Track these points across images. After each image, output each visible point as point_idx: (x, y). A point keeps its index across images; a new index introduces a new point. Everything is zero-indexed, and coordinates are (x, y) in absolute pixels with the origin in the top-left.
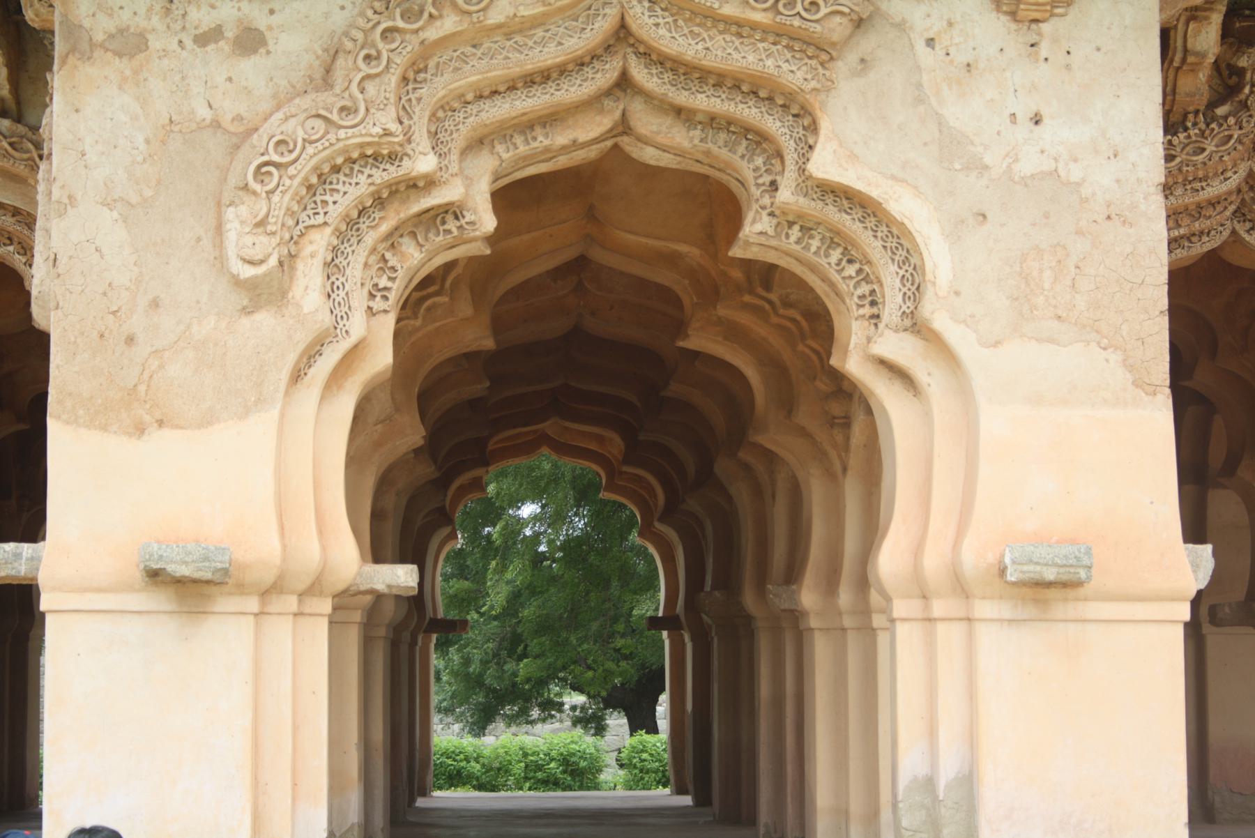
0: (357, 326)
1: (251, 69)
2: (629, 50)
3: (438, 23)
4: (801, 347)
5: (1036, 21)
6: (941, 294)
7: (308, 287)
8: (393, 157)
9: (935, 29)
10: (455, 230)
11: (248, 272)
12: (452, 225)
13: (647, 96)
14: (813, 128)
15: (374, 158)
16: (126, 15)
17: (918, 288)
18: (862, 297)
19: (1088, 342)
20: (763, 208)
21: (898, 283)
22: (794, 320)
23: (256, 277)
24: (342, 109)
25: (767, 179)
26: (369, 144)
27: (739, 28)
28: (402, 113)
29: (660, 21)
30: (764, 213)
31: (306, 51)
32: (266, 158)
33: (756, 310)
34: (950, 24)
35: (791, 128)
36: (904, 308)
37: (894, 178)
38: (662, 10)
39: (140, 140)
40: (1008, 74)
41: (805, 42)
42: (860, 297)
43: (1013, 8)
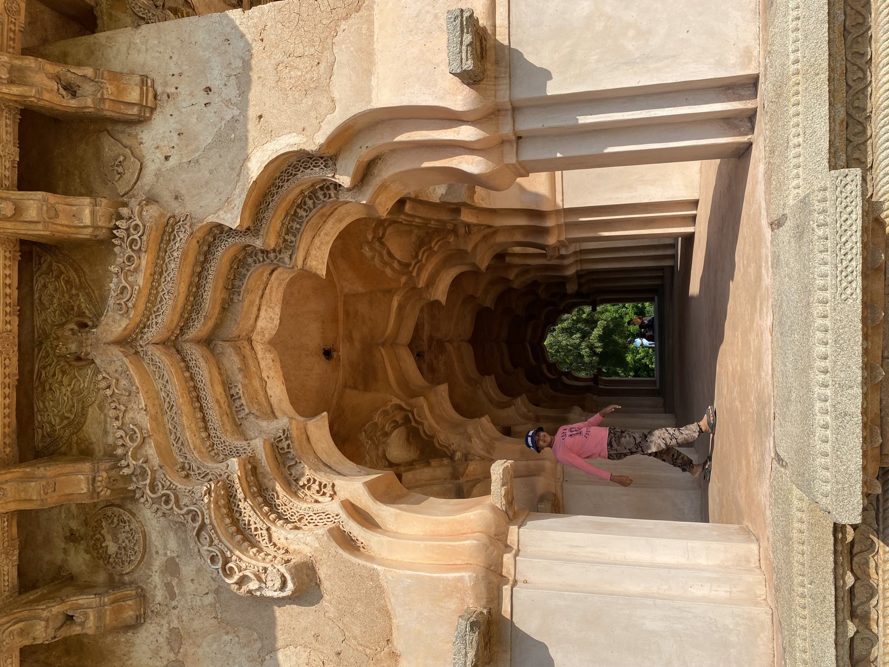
0: (333, 507)
1: (187, 570)
2: (180, 339)
3: (150, 457)
4: (435, 249)
5: (155, 96)
6: (305, 140)
7: (304, 542)
10: (287, 442)
11: (290, 586)
12: (284, 444)
13: (217, 326)
14: (219, 226)
16: (161, 640)
19: (333, 43)
20: (276, 257)
21: (308, 171)
22: (424, 253)
23: (293, 579)
24: (194, 520)
25: (260, 255)
26: (216, 503)
27: (158, 273)
28: (206, 479)
29: (154, 321)
31: (176, 534)
32: (220, 571)
33: (420, 270)
34: (157, 147)
36: (322, 166)
37: (239, 175)
38: (148, 320)
39: (226, 638)
40: (184, 110)
41: (164, 233)
42: (325, 197)
43: (147, 110)
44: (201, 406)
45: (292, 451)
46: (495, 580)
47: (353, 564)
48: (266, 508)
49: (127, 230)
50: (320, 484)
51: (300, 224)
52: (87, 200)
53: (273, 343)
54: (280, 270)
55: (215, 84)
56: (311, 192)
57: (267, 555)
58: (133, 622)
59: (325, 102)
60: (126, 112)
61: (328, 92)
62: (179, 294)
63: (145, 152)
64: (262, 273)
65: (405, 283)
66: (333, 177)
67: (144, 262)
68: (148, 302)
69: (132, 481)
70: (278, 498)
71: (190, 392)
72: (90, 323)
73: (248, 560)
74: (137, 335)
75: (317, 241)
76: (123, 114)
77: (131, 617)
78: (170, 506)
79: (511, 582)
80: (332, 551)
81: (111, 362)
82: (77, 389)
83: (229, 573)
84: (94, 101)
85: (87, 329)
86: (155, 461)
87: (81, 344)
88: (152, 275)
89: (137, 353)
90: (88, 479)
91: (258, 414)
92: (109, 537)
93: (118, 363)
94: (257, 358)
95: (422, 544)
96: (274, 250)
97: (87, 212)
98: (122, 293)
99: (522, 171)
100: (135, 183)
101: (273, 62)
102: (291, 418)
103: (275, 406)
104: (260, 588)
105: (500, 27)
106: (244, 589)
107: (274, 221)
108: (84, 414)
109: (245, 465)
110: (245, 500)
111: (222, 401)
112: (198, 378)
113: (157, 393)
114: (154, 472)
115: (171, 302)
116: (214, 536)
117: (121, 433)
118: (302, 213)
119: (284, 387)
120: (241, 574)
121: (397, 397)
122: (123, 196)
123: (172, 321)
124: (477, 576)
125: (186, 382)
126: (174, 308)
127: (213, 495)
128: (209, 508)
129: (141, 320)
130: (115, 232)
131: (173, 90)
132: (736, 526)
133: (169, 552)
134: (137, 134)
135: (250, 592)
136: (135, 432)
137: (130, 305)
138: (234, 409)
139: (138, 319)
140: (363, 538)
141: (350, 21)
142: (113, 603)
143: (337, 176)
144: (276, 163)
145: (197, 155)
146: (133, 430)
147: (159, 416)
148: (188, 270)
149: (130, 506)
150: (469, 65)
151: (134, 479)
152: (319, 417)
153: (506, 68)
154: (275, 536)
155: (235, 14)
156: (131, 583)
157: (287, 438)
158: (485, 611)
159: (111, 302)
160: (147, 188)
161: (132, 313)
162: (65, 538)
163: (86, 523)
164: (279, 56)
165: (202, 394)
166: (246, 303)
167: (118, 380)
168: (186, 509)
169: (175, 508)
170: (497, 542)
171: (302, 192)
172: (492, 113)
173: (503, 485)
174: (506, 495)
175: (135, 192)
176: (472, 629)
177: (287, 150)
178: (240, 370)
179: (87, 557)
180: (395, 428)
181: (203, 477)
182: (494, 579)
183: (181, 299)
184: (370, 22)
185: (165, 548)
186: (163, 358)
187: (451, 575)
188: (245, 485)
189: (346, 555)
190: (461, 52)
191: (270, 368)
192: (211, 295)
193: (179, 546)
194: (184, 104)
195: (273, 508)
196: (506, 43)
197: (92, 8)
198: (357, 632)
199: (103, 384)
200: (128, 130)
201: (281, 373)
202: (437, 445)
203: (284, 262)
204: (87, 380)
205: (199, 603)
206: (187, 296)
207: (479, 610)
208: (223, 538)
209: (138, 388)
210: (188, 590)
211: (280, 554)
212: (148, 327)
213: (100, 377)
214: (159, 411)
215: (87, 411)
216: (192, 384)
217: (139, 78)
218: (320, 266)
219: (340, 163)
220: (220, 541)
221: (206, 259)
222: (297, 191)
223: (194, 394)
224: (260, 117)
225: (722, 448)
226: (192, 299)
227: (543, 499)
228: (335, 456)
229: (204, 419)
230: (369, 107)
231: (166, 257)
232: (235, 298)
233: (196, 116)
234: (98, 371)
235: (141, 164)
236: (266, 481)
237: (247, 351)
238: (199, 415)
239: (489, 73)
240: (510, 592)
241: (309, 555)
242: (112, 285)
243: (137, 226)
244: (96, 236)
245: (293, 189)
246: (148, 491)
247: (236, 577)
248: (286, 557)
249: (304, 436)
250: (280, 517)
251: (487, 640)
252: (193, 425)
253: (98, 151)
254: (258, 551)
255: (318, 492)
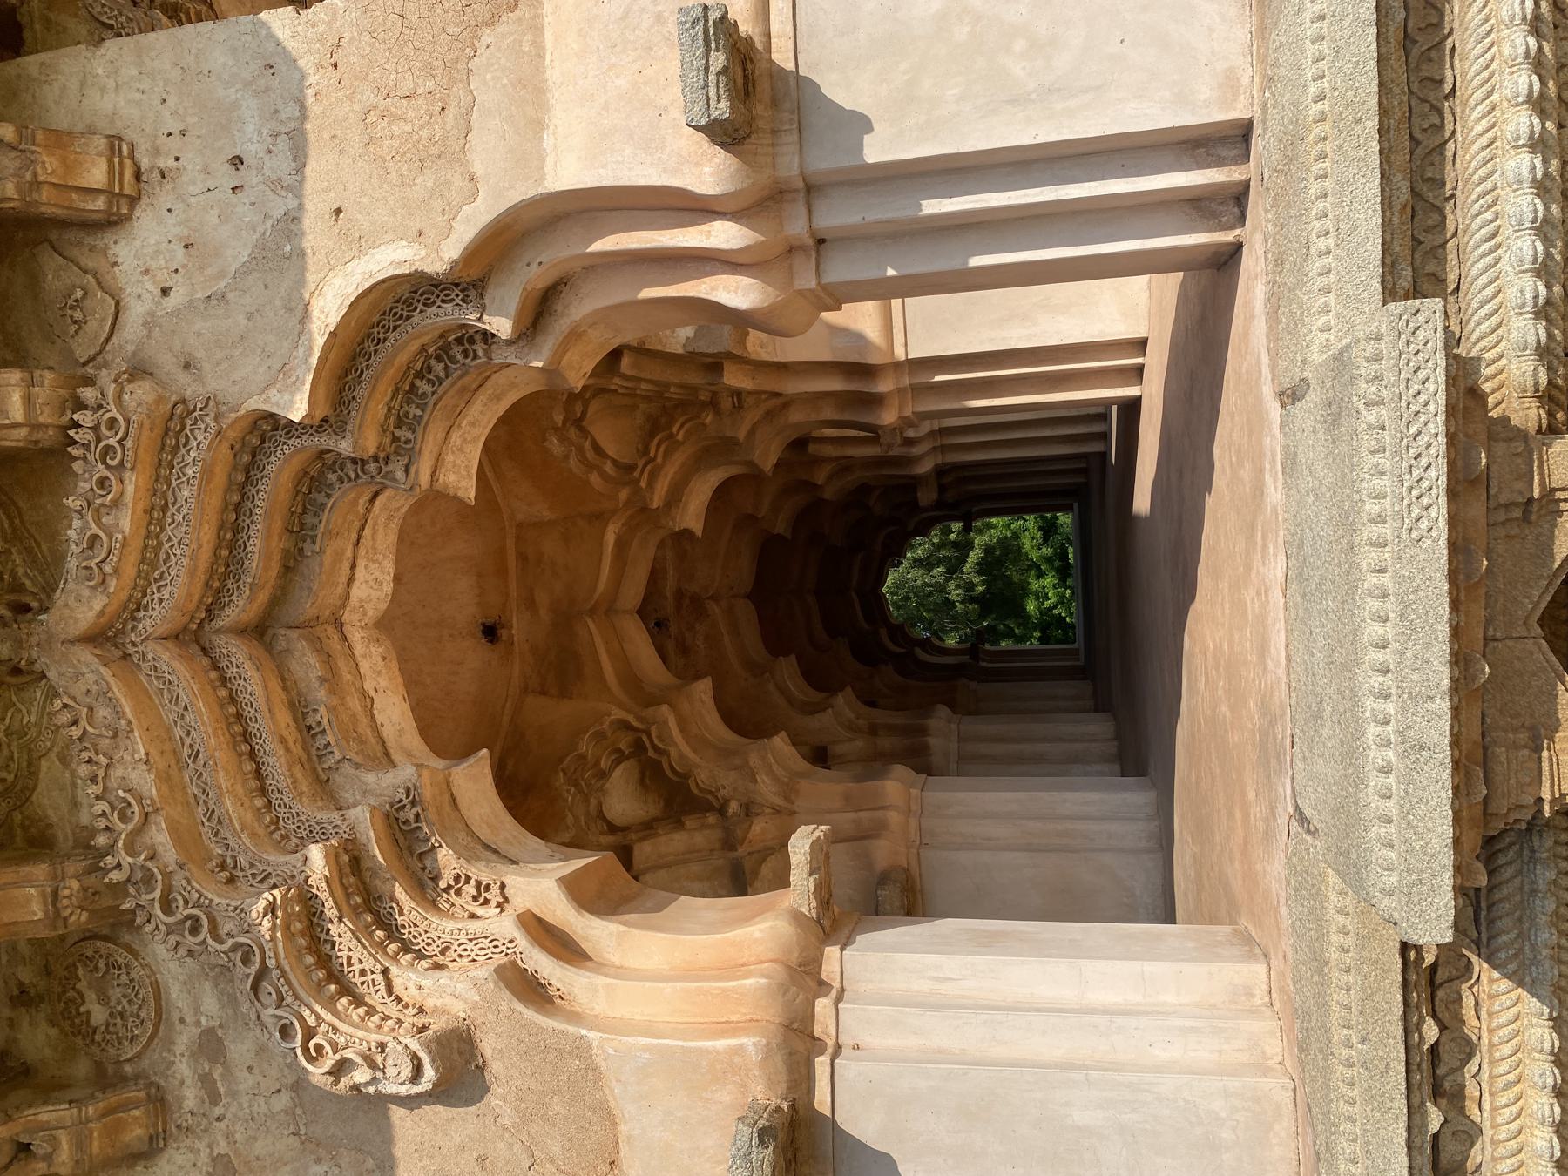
0: (504, 926)
1: (240, 1050)
2: (207, 627)
3: (160, 849)
5: (138, 175)
6: (423, 253)
7: (452, 993)
8: (308, 900)
9: (151, 288)
10: (414, 810)
11: (429, 1073)
12: (410, 814)
13: (276, 601)
14: (271, 417)
15: (308, 923)
17: (436, 286)
18: (466, 353)
19: (469, 71)
23: (433, 1061)
24: (246, 961)
25: (350, 468)
26: (287, 928)
27: (158, 509)
28: (266, 885)
29: (156, 596)
30: (385, 469)
31: (216, 986)
32: (299, 1053)
34: (146, 272)
35: (276, 444)
36: (458, 301)
41: (166, 433)
42: (466, 357)
43: (123, 201)
44: (252, 750)
45: (424, 825)
46: (801, 1048)
47: (543, 1030)
48: (380, 933)
49: (96, 428)
50: (478, 884)
51: (423, 408)
52: (15, 376)
53: (384, 625)
54: (388, 493)
55: (251, 149)
56: (440, 348)
57: (385, 1018)
58: (146, 1148)
59: (458, 181)
60: (82, 205)
61: (463, 163)
62: (200, 546)
63: (122, 281)
64: (356, 500)
65: (628, 502)
66: (479, 319)
67: (130, 489)
68: (142, 561)
69: (127, 894)
70: (401, 914)
71: (229, 725)
72: (35, 604)
73: (351, 1030)
74: (125, 623)
75: (455, 437)
76: (77, 210)
77: (139, 1138)
78: (200, 938)
79: (830, 1050)
80: (504, 1006)
81: (78, 676)
82: (16, 725)
83: (316, 1055)
84: (18, 188)
85: (30, 615)
86: (170, 855)
87: (18, 644)
88: (148, 511)
89: (126, 656)
90: (43, 894)
91: (358, 759)
92: (91, 996)
93: (91, 677)
94: (353, 656)
95: (667, 987)
96: (376, 458)
97: (16, 398)
98: (91, 547)
99: (829, 301)
100: (108, 340)
101: (357, 107)
102: (420, 766)
103: (391, 743)
104: (374, 1080)
105: (779, 37)
106: (345, 1081)
107: (372, 404)
108: (32, 770)
109: (337, 856)
110: (340, 920)
111: (290, 740)
112: (243, 698)
113: (169, 730)
114: (167, 875)
115: (185, 561)
116: (284, 989)
117: (102, 806)
118: (424, 387)
119: (407, 706)
120: (338, 1057)
121: (621, 706)
122: (84, 364)
123: (189, 595)
124: (768, 1044)
125: (222, 706)
126: (192, 573)
127: (279, 913)
128: (273, 939)
129: (131, 596)
130: (72, 433)
131: (171, 162)
132: (1226, 929)
133: (204, 1020)
134: (106, 247)
135: (356, 1087)
136: (129, 804)
137: (108, 568)
138: (314, 752)
139: (124, 596)
140: (559, 980)
141: (500, 29)
142: (104, 1115)
143: (485, 317)
144: (371, 297)
145: (222, 284)
146: (125, 800)
147: (174, 772)
148: (215, 501)
149: (127, 938)
150: (722, 109)
151: (132, 890)
152: (472, 760)
153: (792, 112)
154: (398, 984)
155: (280, 21)
156: (137, 1077)
157: (413, 803)
158: (785, 1106)
159: (72, 564)
160: (130, 348)
161: (112, 584)
162: (11, 999)
163: (47, 972)
164: (368, 97)
165: (253, 728)
166: (328, 557)
167: (91, 709)
168: (230, 942)
169: (209, 941)
170: (804, 978)
171: (423, 349)
172: (770, 198)
173: (811, 874)
174: (818, 890)
175: (109, 357)
176: (761, 1141)
177: (391, 272)
178: (322, 680)
179: (54, 1032)
180: (617, 762)
181: (261, 882)
182: (799, 1045)
183: (205, 555)
184: (538, 30)
185: (197, 1010)
186: (176, 664)
187: (721, 1044)
188: (339, 893)
189: (529, 1014)
190: (706, 86)
191: (379, 673)
192: (262, 545)
193: (223, 1007)
194: (192, 189)
195: (393, 932)
196: (790, 66)
197: (13, 9)
198: (556, 1150)
199: (65, 717)
200: (89, 240)
201: (400, 680)
202: (696, 791)
203: (395, 480)
204: (34, 710)
205: (264, 1108)
206: (217, 548)
207: (773, 1106)
208: (302, 993)
209: (130, 723)
210: (241, 1087)
211: (409, 1017)
212: (146, 609)
213: (58, 704)
214: (173, 762)
215: (39, 768)
216: (232, 710)
217: (103, 141)
218: (463, 483)
219: (493, 294)
220: (297, 997)
221: (248, 478)
222: (414, 347)
223: (238, 728)
224: (338, 211)
225: (1198, 783)
226: (225, 553)
227: (885, 892)
228: (507, 830)
229: (258, 774)
230: (541, 190)
231: (173, 478)
232: (307, 547)
233: (215, 212)
234: (53, 694)
235: (117, 304)
236: (377, 882)
237: (335, 644)
238: (249, 766)
239: (760, 122)
240: (828, 1069)
241: (463, 1015)
242: (71, 533)
243: (113, 421)
244: (36, 442)
245: (407, 343)
246: (159, 912)
247: (329, 1062)
248: (420, 1021)
249: (447, 797)
250: (406, 947)
251: (790, 1155)
252: (238, 787)
253: (34, 281)
254: (367, 1013)
255: (475, 899)
